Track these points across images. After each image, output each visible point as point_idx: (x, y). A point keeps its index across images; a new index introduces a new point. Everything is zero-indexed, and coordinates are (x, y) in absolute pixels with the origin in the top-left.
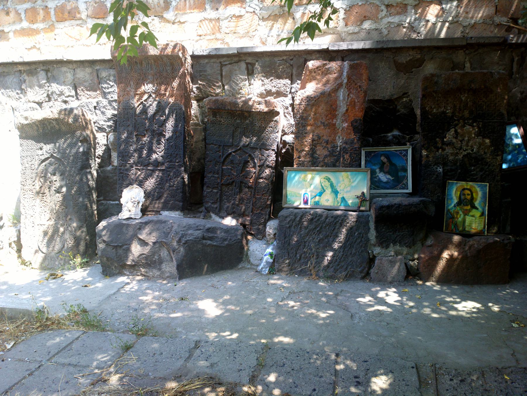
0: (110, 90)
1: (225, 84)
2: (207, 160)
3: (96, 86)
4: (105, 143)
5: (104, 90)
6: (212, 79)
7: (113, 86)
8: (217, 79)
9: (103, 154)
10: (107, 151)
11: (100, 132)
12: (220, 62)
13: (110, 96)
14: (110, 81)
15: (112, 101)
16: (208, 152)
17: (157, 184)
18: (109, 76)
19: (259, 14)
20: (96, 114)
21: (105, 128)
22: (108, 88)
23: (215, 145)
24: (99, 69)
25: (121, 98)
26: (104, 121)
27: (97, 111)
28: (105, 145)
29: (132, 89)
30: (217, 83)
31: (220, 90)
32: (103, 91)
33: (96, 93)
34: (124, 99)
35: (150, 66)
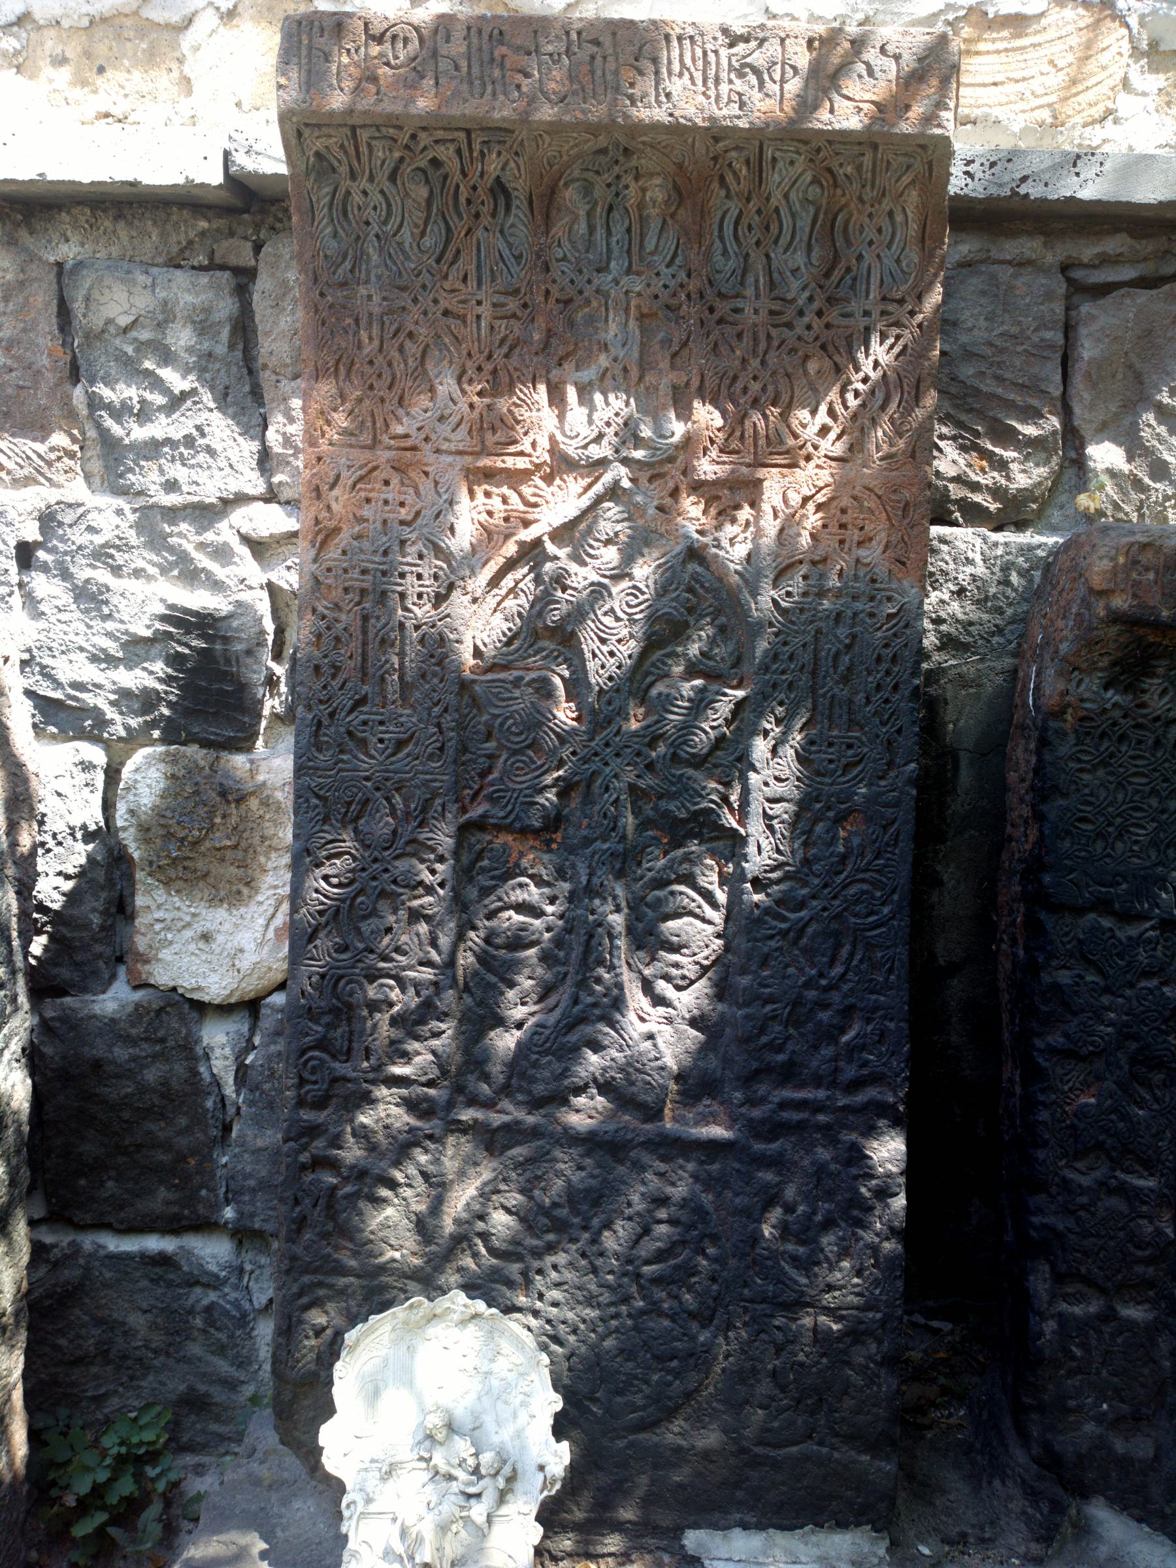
0: (160, 428)
1: (1086, 430)
2: (1056, 1039)
3: (44, 387)
4: (93, 816)
5: (109, 423)
6: (988, 386)
7: (184, 395)
8: (1033, 387)
9: (71, 898)
10: (100, 875)
11: (53, 737)
12: (1065, 268)
13: (154, 476)
14: (166, 357)
15: (172, 514)
16: (1065, 977)
17: (657, 1280)
18: (165, 317)
19: (1133, 21)
20: (31, 602)
21: (96, 713)
22: (144, 414)
23: (1127, 917)
24: (79, 265)
25: (340, 500)
26: (94, 659)
27: (40, 584)
28: (89, 837)
29: (445, 429)
30: (1032, 415)
31: (1043, 471)
32: (104, 434)
33: (41, 448)
34: (366, 512)
35: (618, 231)
